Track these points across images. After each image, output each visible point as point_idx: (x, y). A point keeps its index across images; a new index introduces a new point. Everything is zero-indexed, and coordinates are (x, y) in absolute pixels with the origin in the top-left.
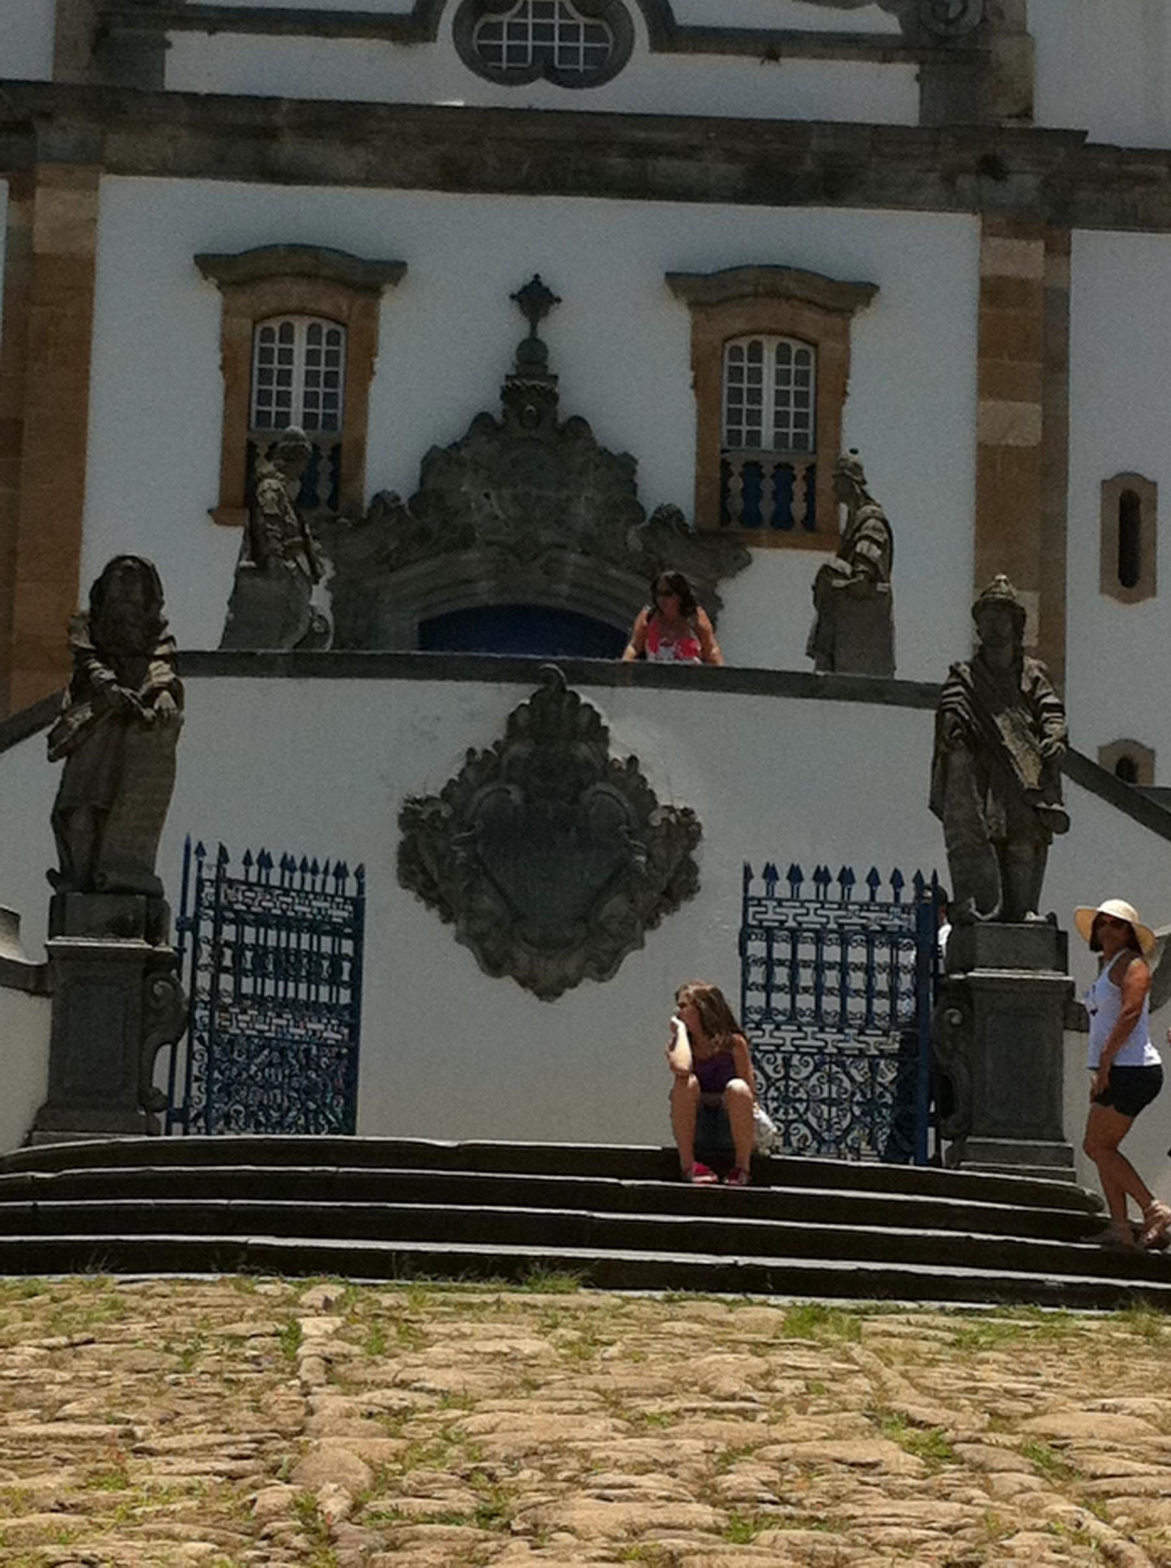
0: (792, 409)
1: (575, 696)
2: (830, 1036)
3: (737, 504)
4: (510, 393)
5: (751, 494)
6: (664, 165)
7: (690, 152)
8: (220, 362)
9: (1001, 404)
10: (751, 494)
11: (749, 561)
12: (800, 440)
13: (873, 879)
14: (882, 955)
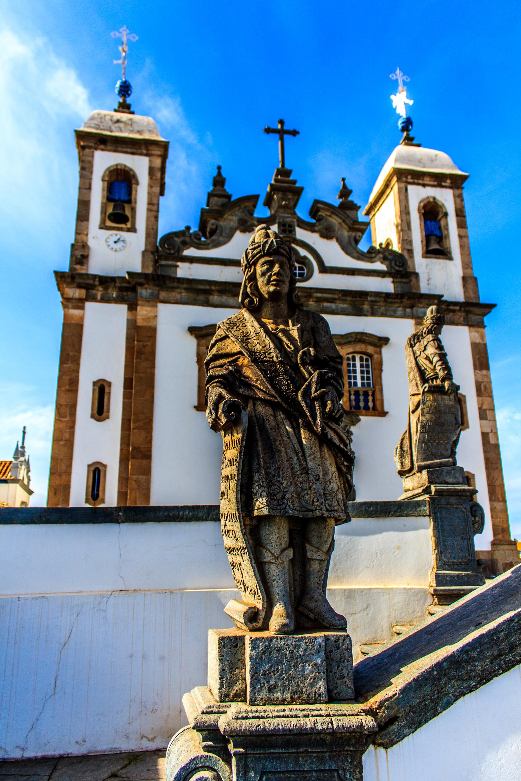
0: (365, 375)
3: (354, 403)
5: (357, 400)
6: (325, 304)
7: (332, 301)
8: (195, 359)
10: (357, 400)
11: (359, 420)
12: (369, 384)
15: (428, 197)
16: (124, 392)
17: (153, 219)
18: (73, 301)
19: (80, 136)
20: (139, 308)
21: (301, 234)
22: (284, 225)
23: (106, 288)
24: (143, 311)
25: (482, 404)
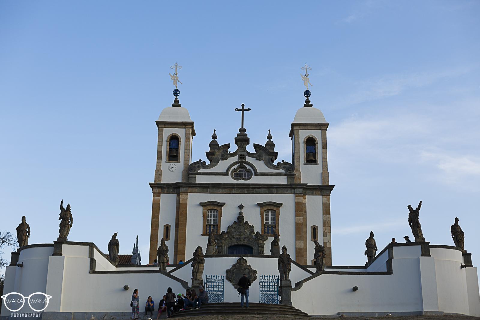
1: (244, 258)
2: (268, 292)
3: (267, 231)
4: (238, 218)
5: (268, 230)
6: (257, 189)
9: (299, 218)
10: (268, 230)
13: (272, 277)
14: (273, 284)
15: (309, 135)
16: (175, 229)
17: (187, 156)
18: (156, 194)
19: (158, 123)
20: (181, 196)
21: (248, 159)
22: (241, 155)
23: (168, 188)
24: (182, 197)
25: (325, 230)
